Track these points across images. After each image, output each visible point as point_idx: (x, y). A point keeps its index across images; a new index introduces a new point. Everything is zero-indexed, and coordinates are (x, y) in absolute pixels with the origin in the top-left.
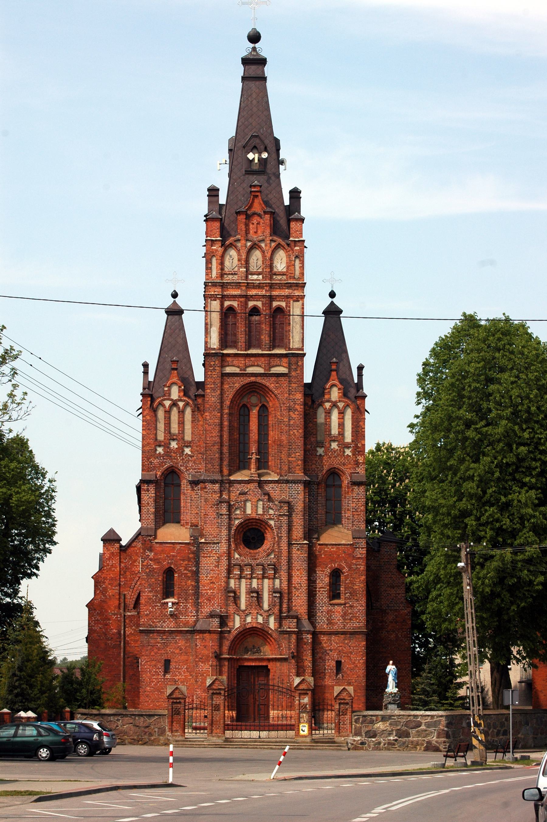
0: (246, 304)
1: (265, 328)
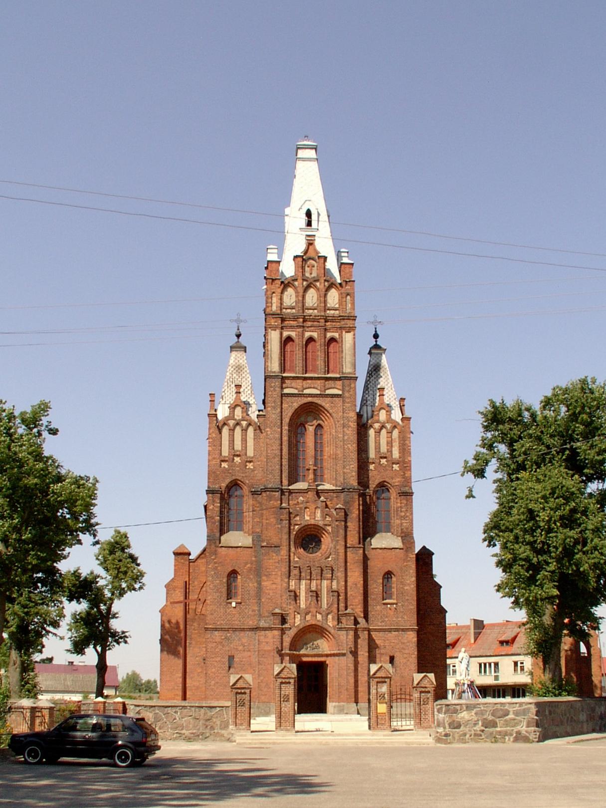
0: (303, 334)
1: (320, 355)
